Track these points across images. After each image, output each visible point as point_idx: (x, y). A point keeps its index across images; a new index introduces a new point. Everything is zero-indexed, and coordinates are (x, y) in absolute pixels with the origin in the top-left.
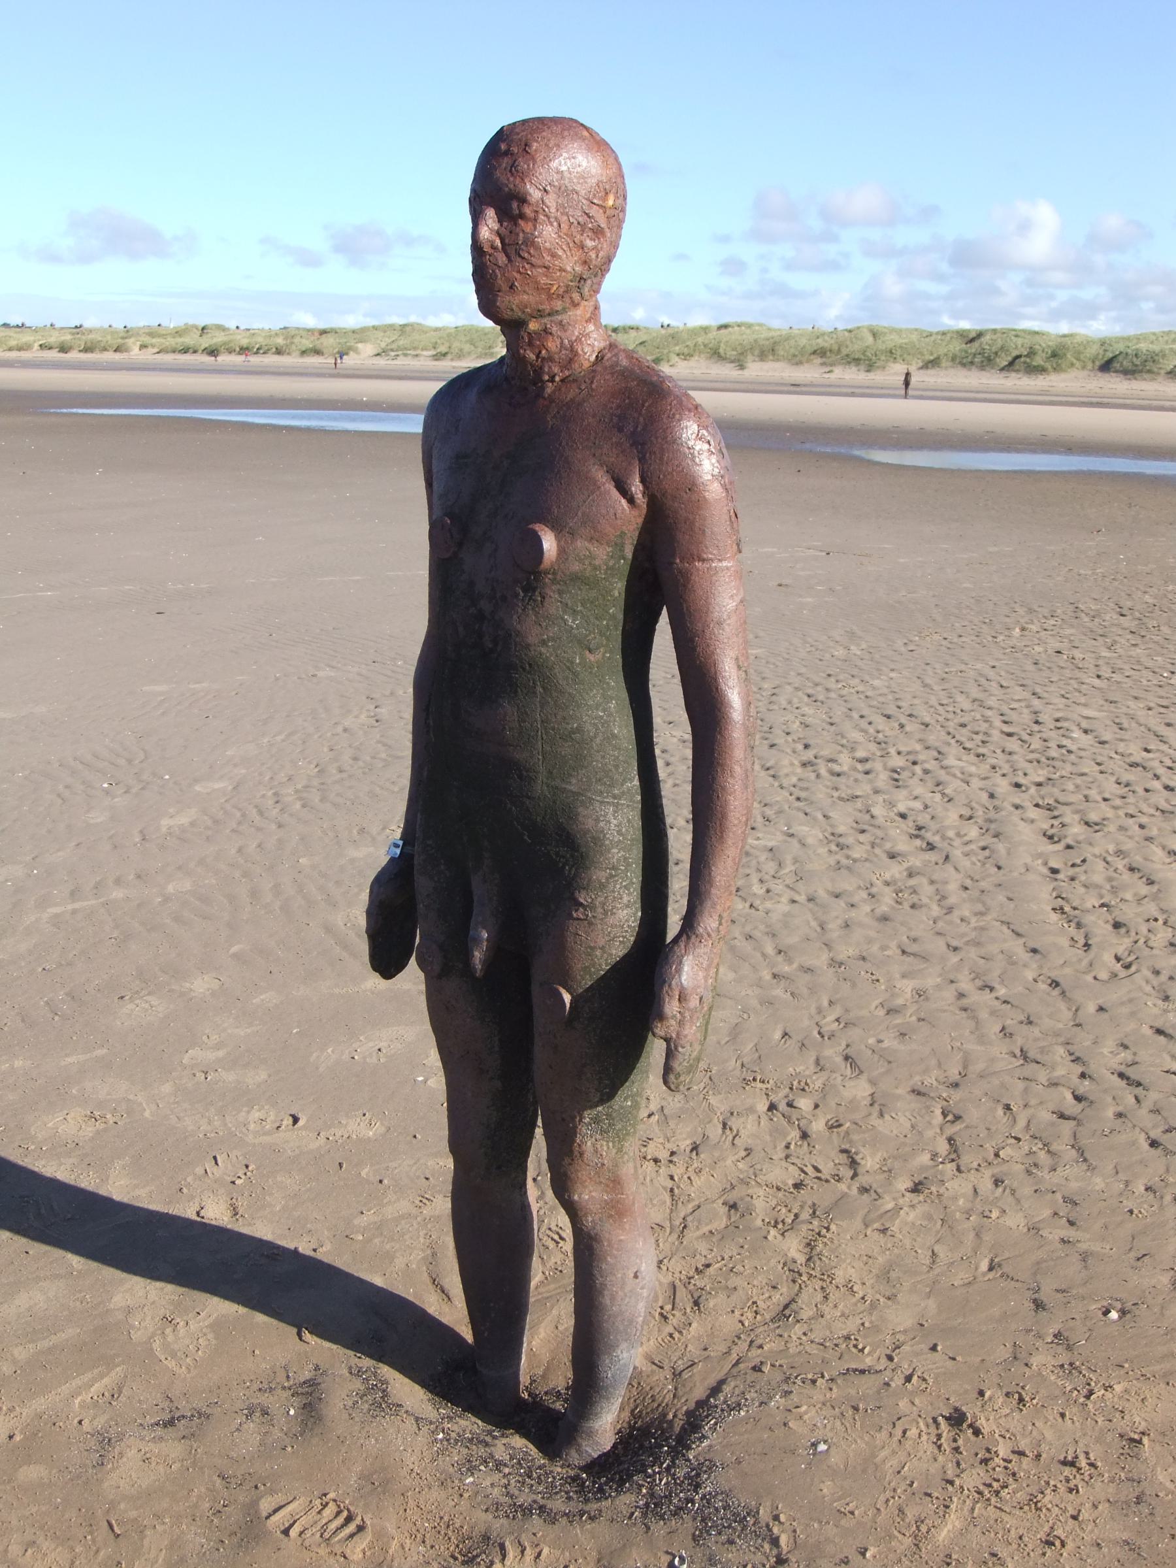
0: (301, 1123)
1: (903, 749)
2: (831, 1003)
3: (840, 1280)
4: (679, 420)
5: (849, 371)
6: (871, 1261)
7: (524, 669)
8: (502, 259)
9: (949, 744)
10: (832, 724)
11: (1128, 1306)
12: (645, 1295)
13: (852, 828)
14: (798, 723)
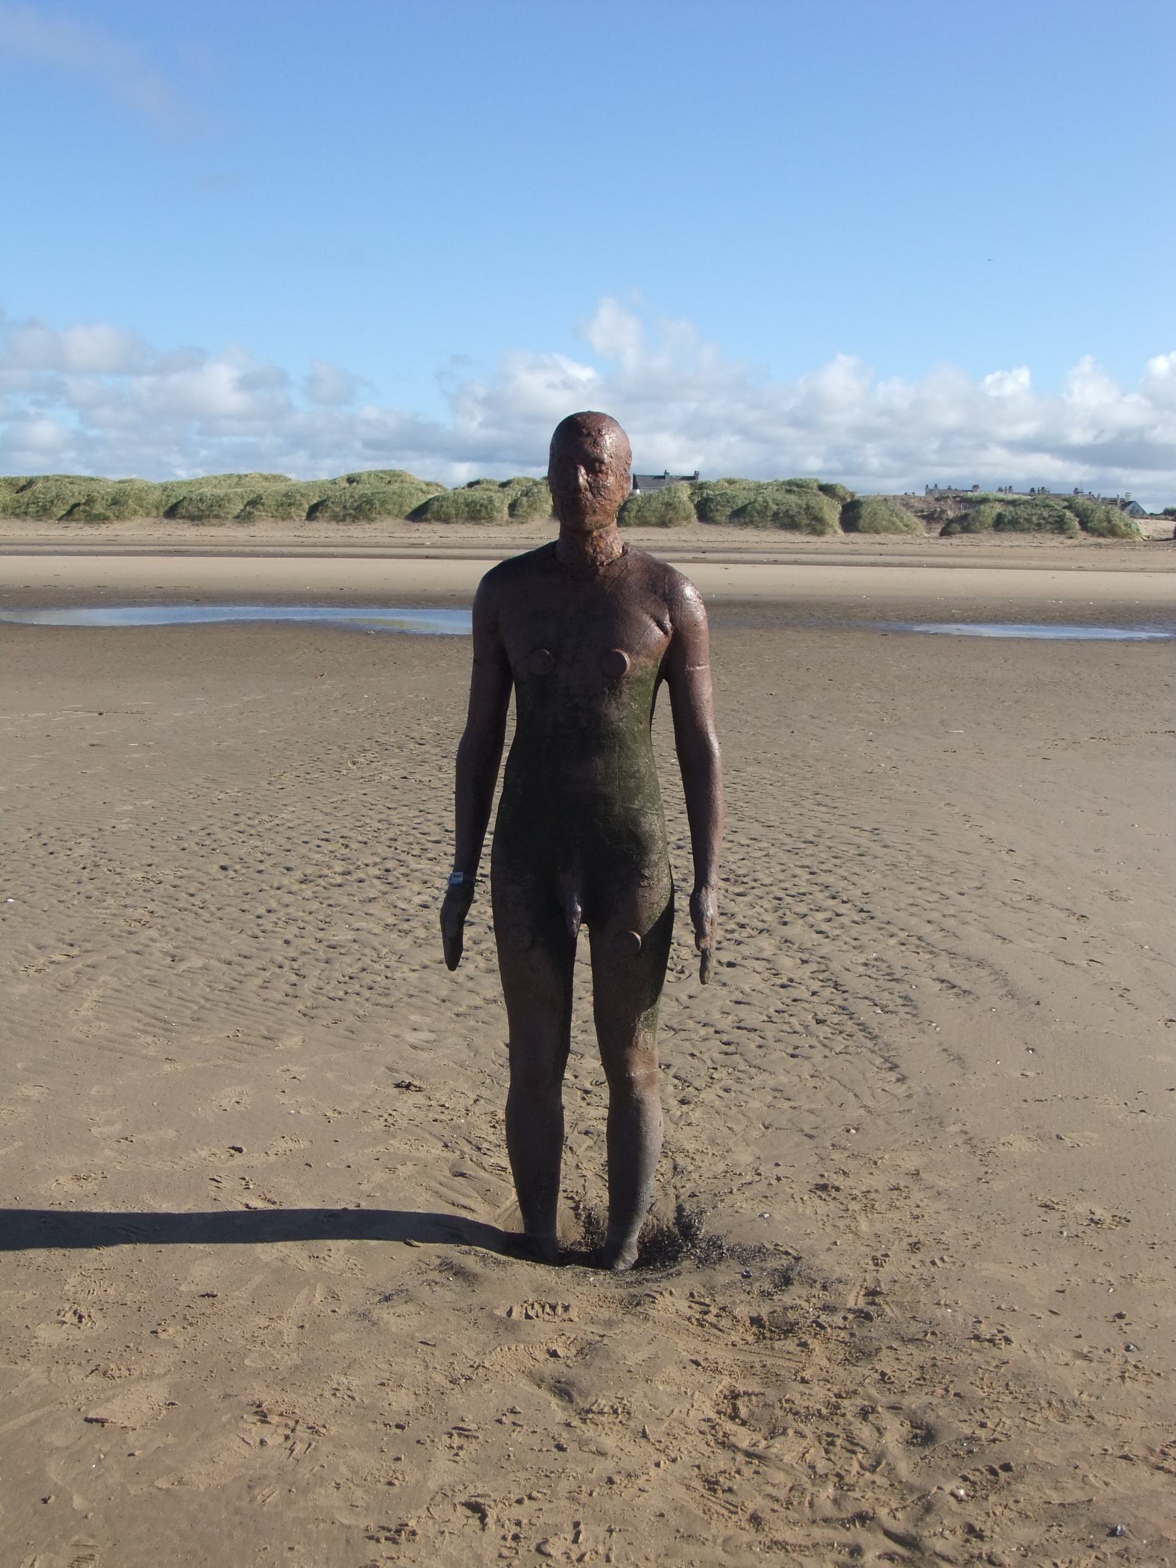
8: (589, 495)
11: (855, 1126)
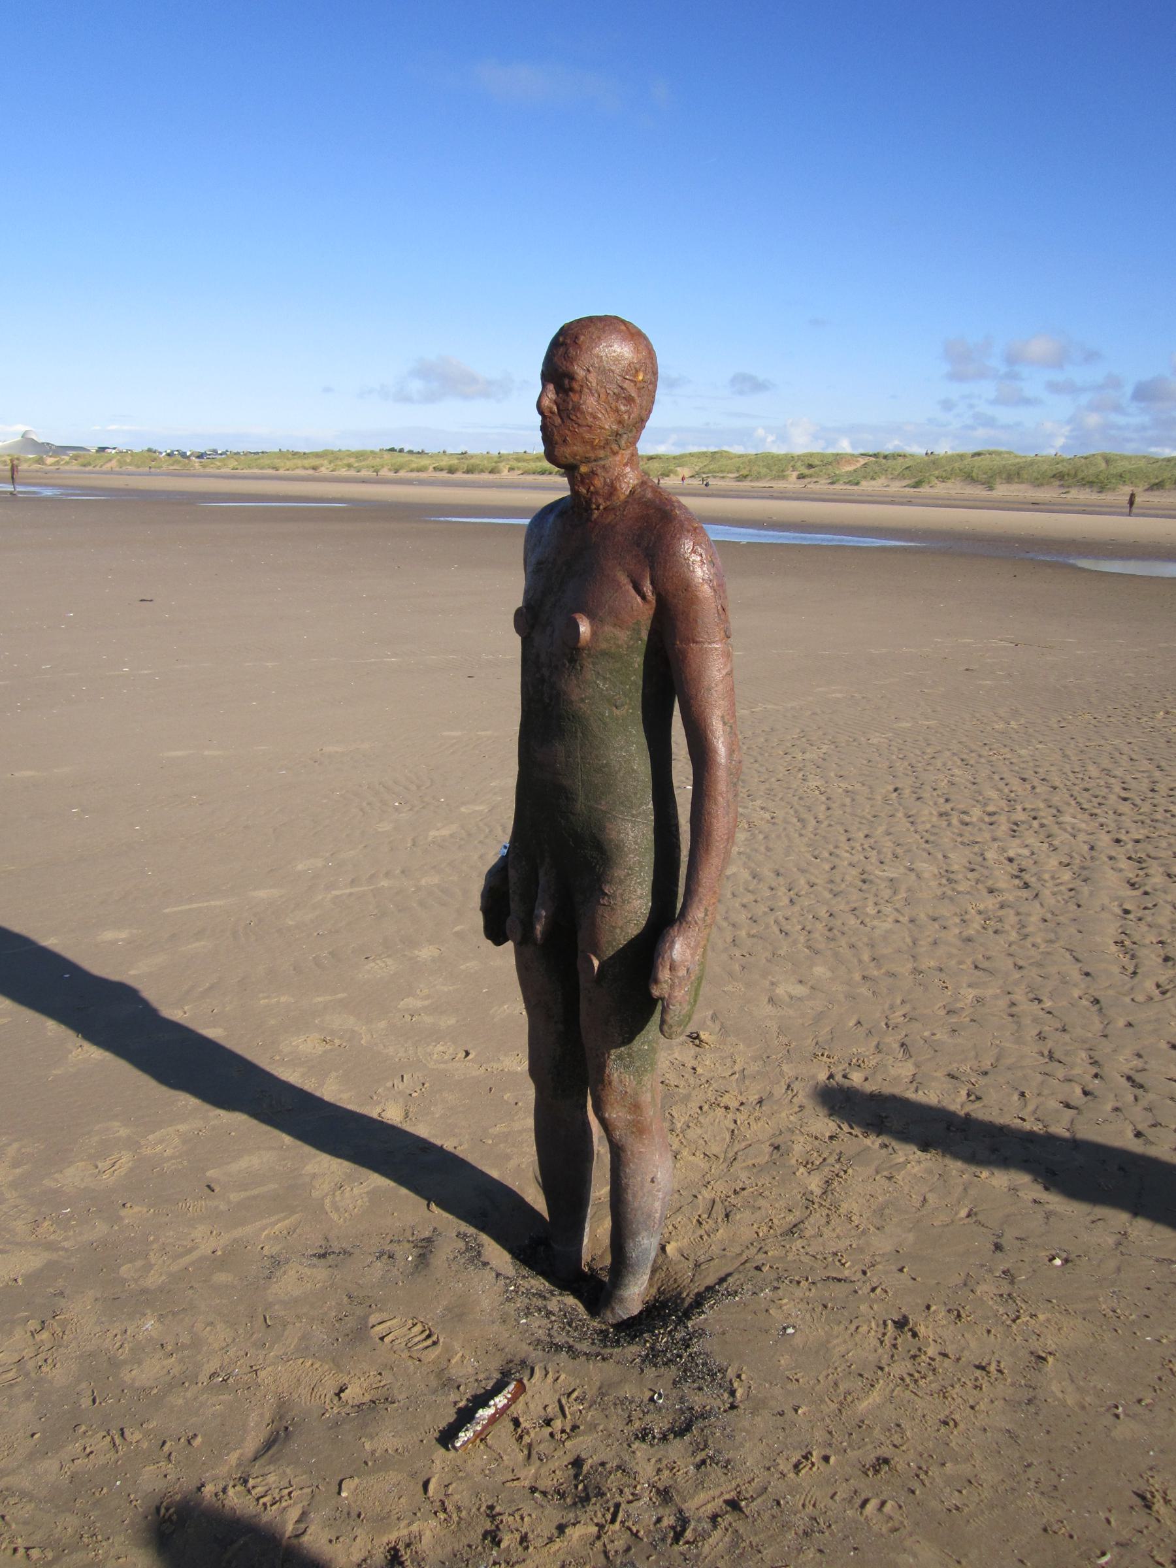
0: (470, 1057)
1: (1028, 806)
2: (903, 1002)
3: (842, 1211)
4: (679, 539)
6: (872, 1199)
7: (569, 719)
8: (558, 421)
9: (1069, 804)
10: (974, 784)
11: (1073, 1256)
12: (661, 1196)
13: (965, 867)
14: (946, 781)
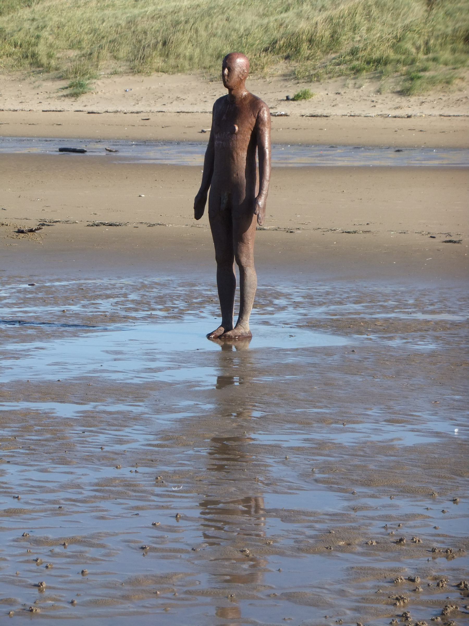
5: (355, 93)
